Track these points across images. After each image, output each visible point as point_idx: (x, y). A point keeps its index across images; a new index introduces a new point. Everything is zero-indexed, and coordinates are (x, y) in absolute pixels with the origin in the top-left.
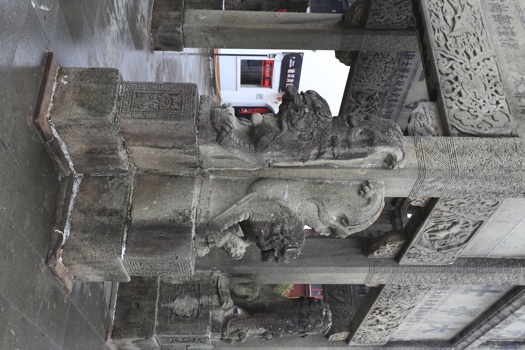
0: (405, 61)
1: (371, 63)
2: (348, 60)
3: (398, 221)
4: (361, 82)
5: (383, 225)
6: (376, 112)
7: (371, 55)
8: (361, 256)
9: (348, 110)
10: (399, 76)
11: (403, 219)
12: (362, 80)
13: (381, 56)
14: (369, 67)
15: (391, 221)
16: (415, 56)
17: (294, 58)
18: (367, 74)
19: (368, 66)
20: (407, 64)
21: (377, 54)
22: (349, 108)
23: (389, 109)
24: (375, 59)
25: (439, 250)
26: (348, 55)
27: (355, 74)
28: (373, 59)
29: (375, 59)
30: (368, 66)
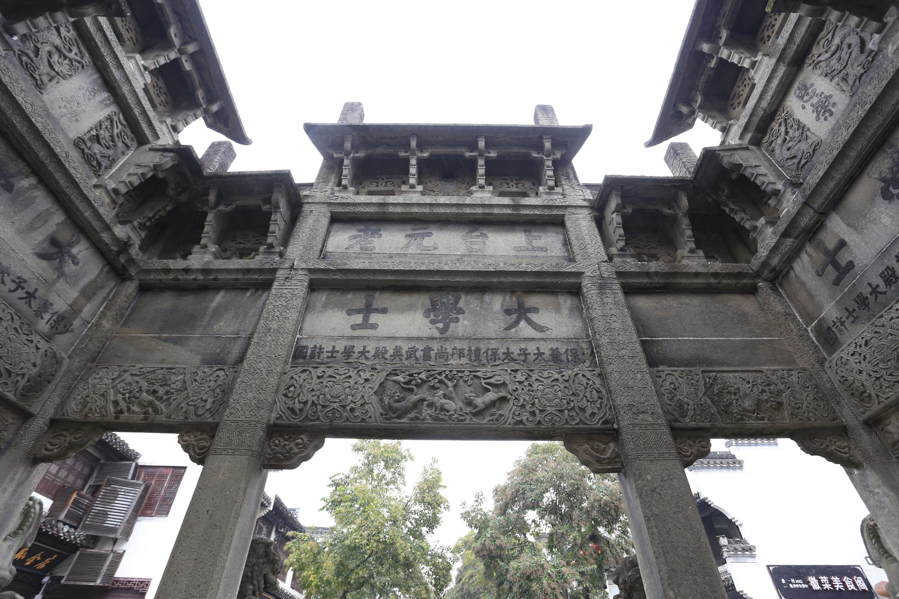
0: (325, 355)
1: (305, 400)
2: (299, 441)
3: (775, 261)
4: (352, 410)
5: (803, 278)
6: (451, 371)
7: (286, 403)
9: (443, 420)
10: (363, 357)
11: (764, 254)
12: (348, 408)
13: (292, 389)
14: (313, 402)
15: (788, 272)
16: (315, 345)
17: (783, 581)
19: (310, 403)
20: (333, 351)
22: (436, 419)
23: (453, 355)
27: (331, 421)
29: (295, 396)
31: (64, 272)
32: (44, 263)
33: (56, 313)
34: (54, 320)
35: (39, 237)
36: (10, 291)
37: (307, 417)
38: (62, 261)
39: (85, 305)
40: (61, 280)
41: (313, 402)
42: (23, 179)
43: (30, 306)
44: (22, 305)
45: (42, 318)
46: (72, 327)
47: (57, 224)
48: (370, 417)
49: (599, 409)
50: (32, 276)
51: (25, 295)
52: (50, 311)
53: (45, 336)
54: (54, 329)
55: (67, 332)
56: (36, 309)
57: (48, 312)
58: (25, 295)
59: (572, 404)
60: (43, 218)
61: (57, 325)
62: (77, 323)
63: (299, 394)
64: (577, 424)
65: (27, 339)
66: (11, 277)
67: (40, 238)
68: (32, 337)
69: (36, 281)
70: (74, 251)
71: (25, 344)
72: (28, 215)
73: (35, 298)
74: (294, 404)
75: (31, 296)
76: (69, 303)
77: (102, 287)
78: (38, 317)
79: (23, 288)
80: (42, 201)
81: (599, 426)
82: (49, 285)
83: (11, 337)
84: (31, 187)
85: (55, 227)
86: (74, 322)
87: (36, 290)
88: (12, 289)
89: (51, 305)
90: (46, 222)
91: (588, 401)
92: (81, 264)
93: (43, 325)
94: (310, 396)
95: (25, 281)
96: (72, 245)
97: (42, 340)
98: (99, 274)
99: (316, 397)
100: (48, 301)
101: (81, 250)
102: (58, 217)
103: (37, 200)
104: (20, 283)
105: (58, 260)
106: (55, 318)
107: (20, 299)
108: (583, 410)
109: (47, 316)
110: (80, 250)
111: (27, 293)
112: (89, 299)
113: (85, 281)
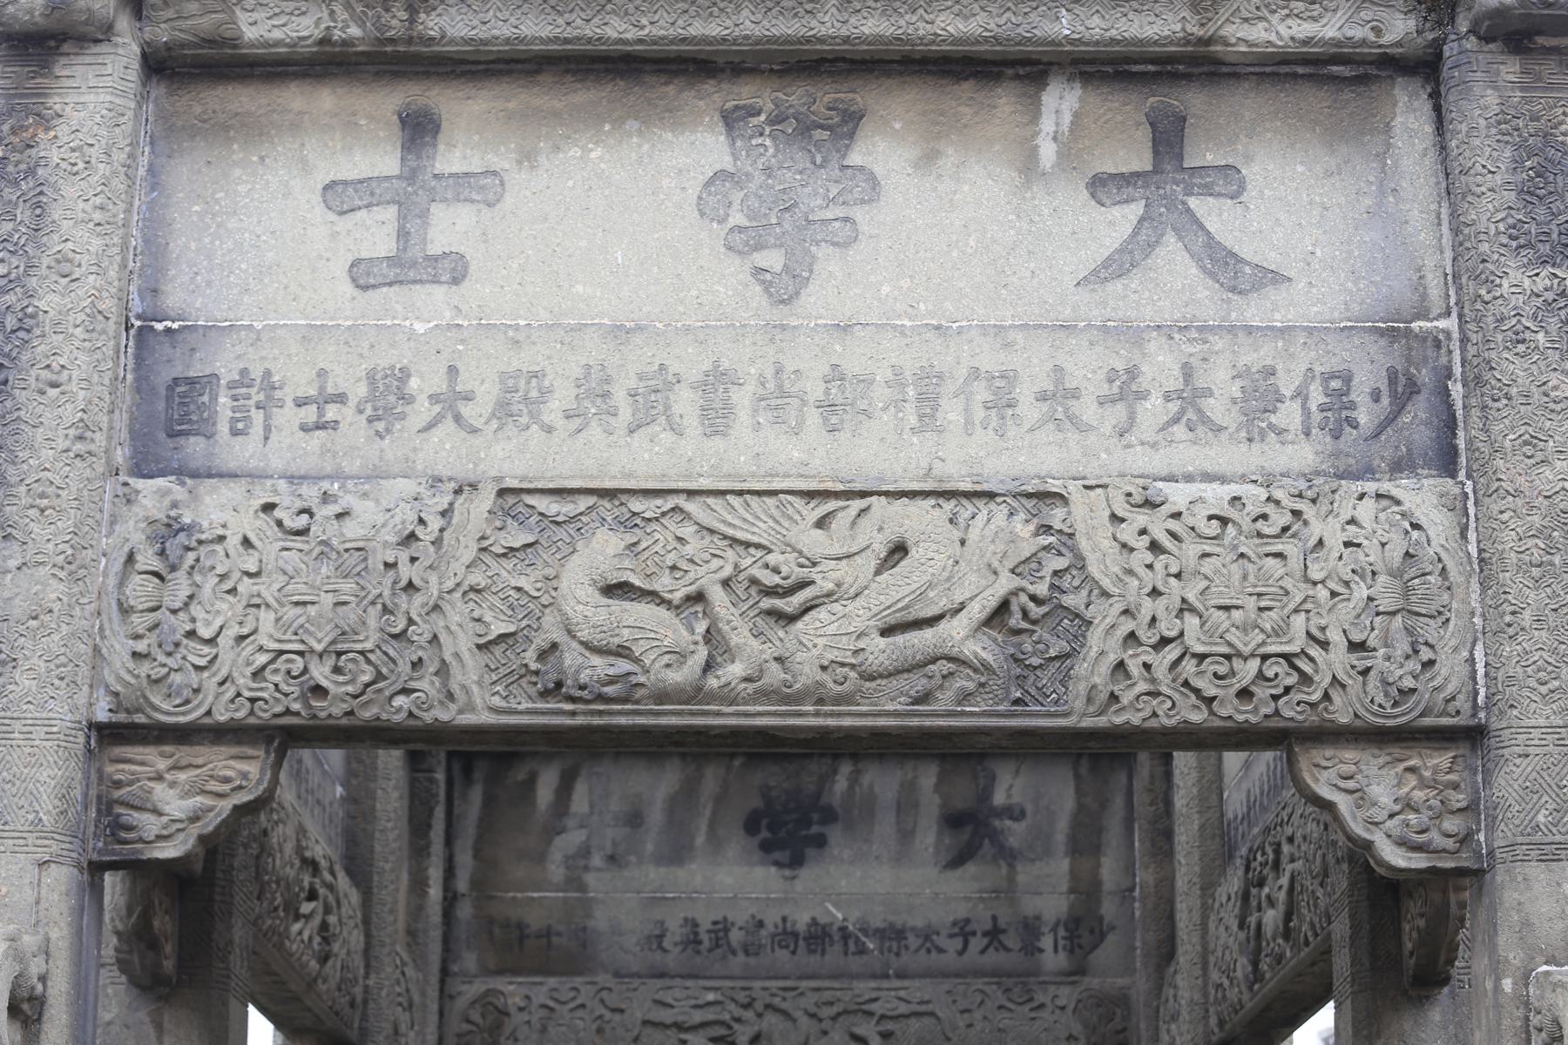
31: (1012, 849)
32: (971, 868)
33: (1057, 924)
34: (1064, 938)
35: (928, 836)
36: (961, 953)
38: (995, 836)
39: (1099, 865)
40: (1019, 867)
42: (834, 782)
43: (1007, 949)
44: (994, 958)
45: (1041, 951)
46: (1105, 922)
47: (937, 788)
50: (970, 905)
51: (985, 941)
52: (1045, 929)
53: (1070, 974)
54: (1077, 950)
55: (1103, 936)
56: (1019, 946)
57: (1043, 934)
58: (985, 941)
60: (907, 805)
61: (1076, 941)
62: (1109, 909)
65: (1031, 1010)
66: (944, 932)
67: (931, 838)
68: (1040, 998)
69: (981, 906)
70: (999, 798)
71: (1034, 1019)
72: (886, 825)
73: (1004, 931)
75: (994, 934)
76: (1065, 888)
77: (1104, 804)
78: (1032, 954)
79: (974, 933)
80: (883, 782)
82: (1007, 891)
83: (1001, 1026)
84: (854, 779)
85: (937, 800)
86: (1103, 911)
87: (994, 918)
88: (960, 947)
89: (1038, 918)
90: (916, 805)
92: (1029, 808)
93: (1053, 958)
95: (967, 921)
96: (986, 794)
97: (1062, 987)
98: (1079, 791)
100: (1026, 918)
101: (1009, 786)
102: (928, 777)
103: (877, 790)
104: (963, 930)
105: (986, 841)
106: (1062, 932)
107: (983, 951)
109: (1047, 942)
110: (1006, 785)
111: (985, 934)
112: (1096, 850)
113: (1062, 826)
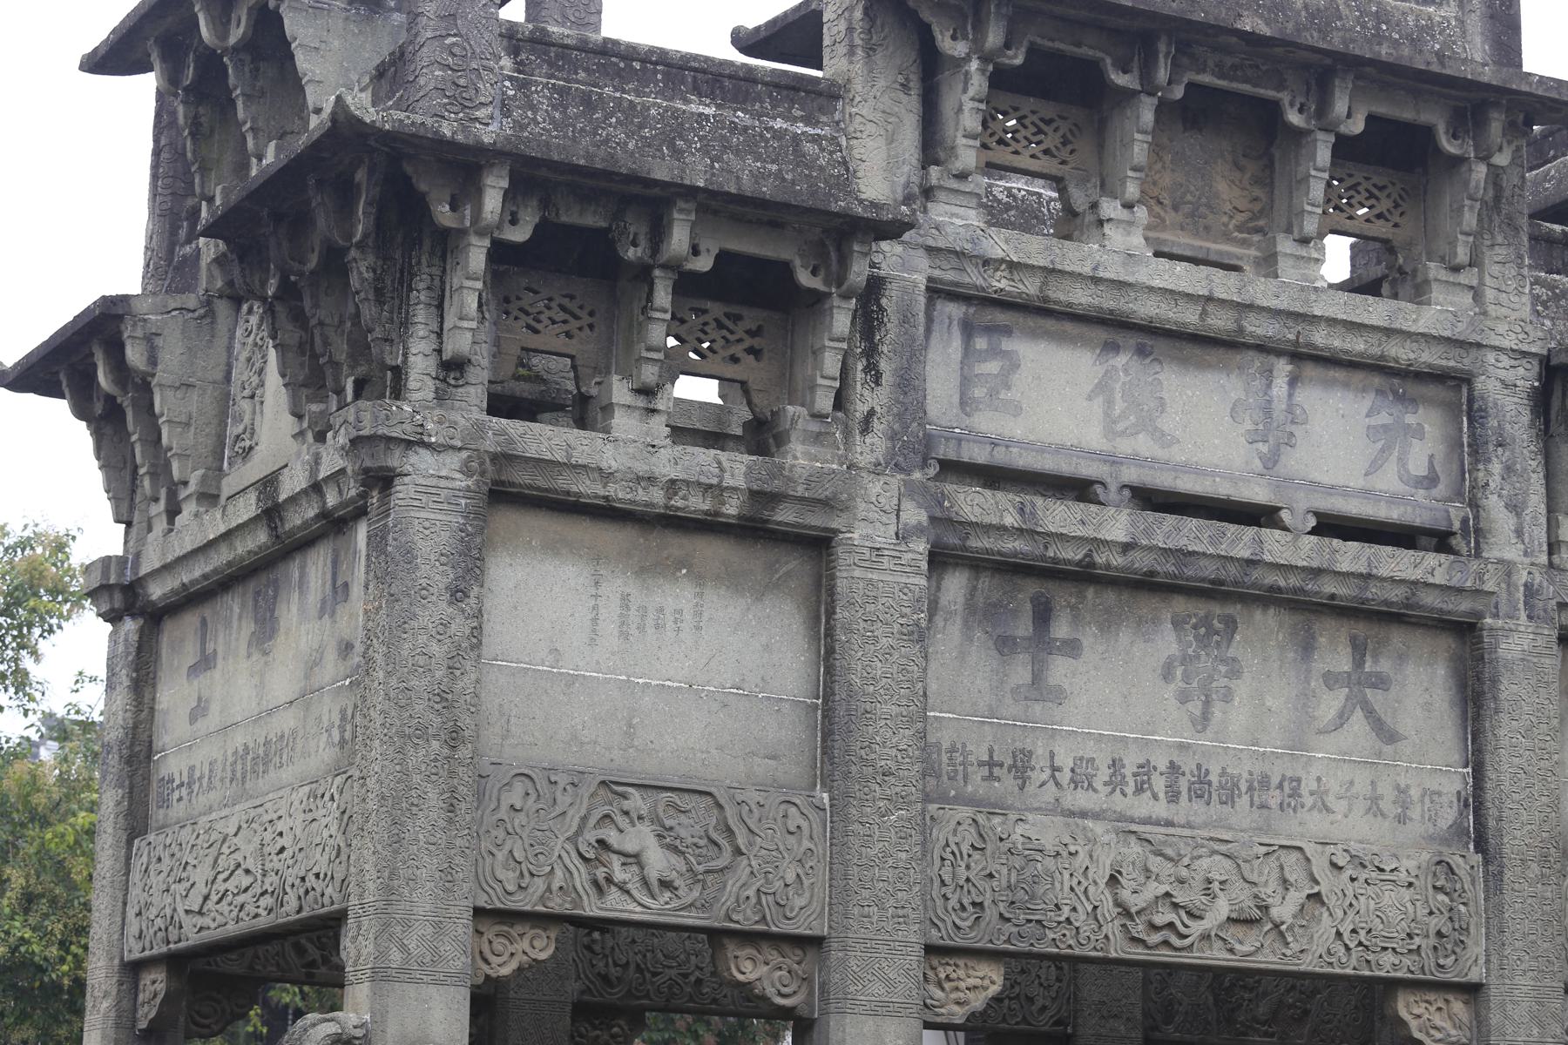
2: (616, 1030)
4: (699, 982)
7: (593, 966)
8: (816, 1029)
12: (693, 979)
14: (638, 965)
18: (665, 966)
19: (632, 967)
21: (589, 948)
24: (607, 952)
25: (738, 852)
26: (598, 1032)
27: (667, 1000)
28: (606, 956)
29: (607, 952)
30: (632, 967)
37: (629, 991)
41: (638, 965)
48: (725, 996)
49: (1054, 999)
59: (1017, 989)
63: (613, 948)
64: (1017, 1023)
74: (607, 965)
81: (1046, 1028)
91: (1041, 985)
94: (631, 954)
99: (640, 956)
108: (1031, 1000)
